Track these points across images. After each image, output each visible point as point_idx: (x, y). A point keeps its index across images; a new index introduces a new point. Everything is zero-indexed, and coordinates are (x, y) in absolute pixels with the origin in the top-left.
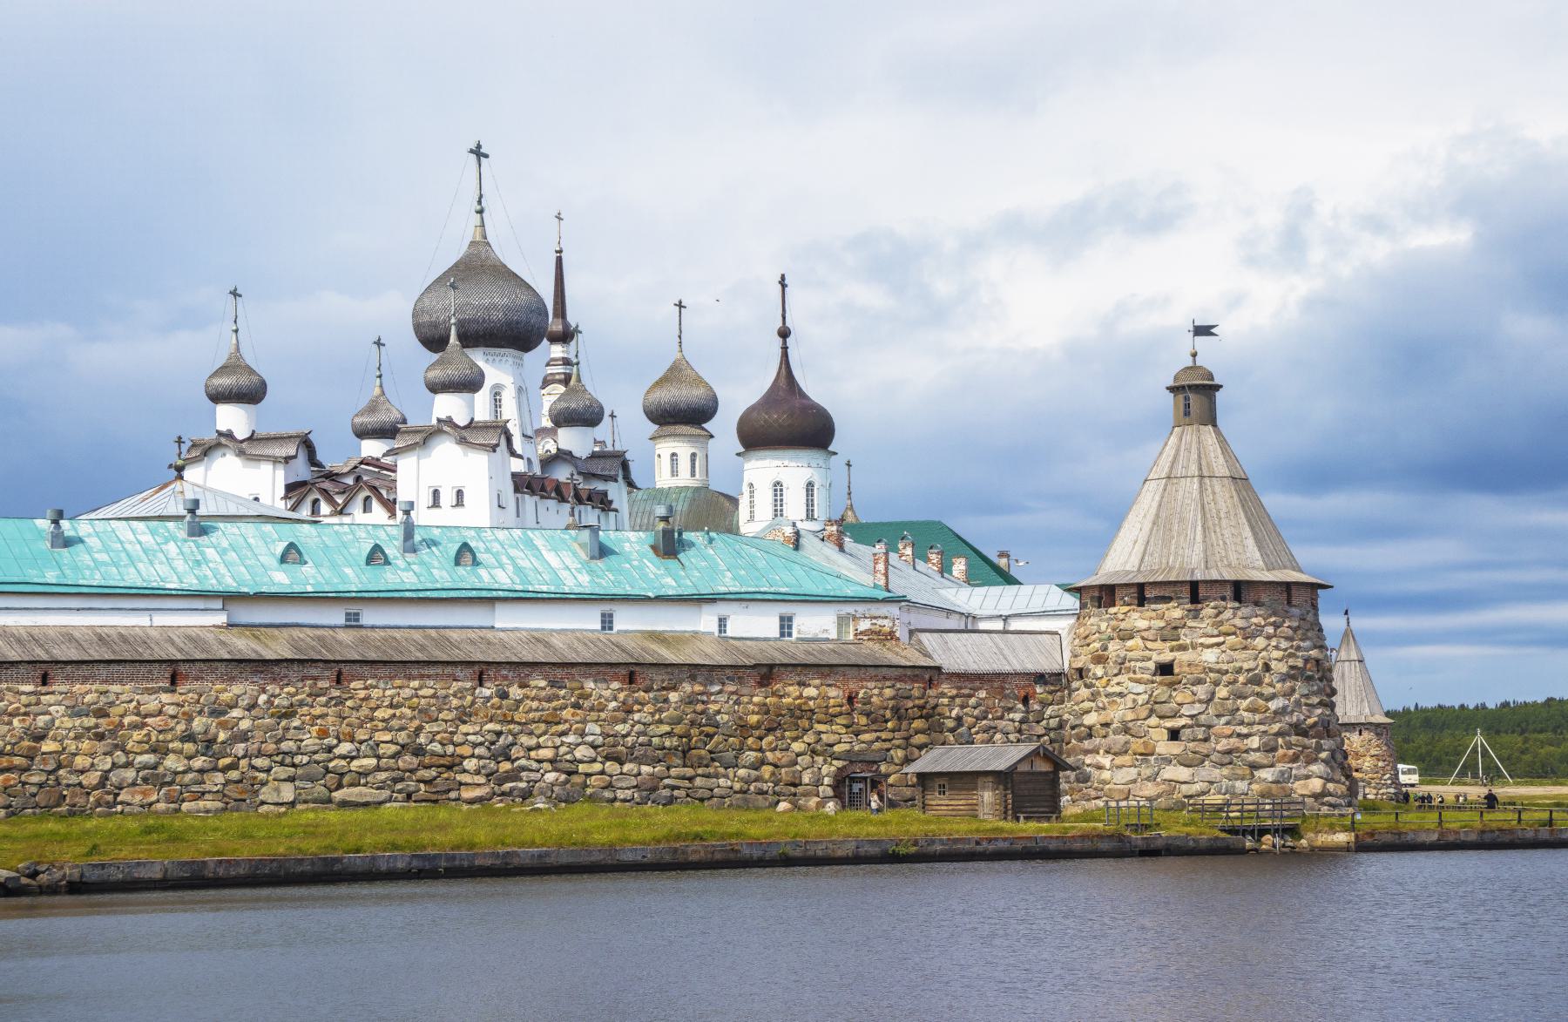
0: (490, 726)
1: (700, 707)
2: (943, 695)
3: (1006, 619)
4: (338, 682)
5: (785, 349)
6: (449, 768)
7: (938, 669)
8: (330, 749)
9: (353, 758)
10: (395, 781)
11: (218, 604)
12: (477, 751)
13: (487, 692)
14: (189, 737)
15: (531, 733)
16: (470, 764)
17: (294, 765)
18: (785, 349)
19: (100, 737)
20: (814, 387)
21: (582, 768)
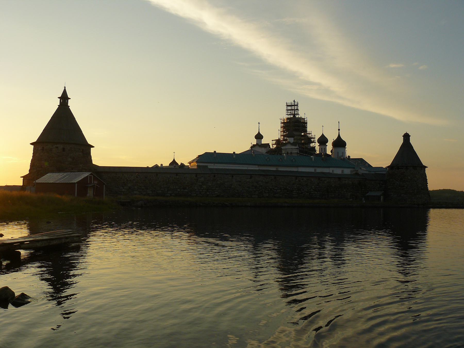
0: (298, 186)
4: (275, 178)
5: (339, 132)
8: (273, 188)
9: (277, 190)
11: (257, 166)
13: (297, 180)
18: (339, 132)
19: (240, 185)
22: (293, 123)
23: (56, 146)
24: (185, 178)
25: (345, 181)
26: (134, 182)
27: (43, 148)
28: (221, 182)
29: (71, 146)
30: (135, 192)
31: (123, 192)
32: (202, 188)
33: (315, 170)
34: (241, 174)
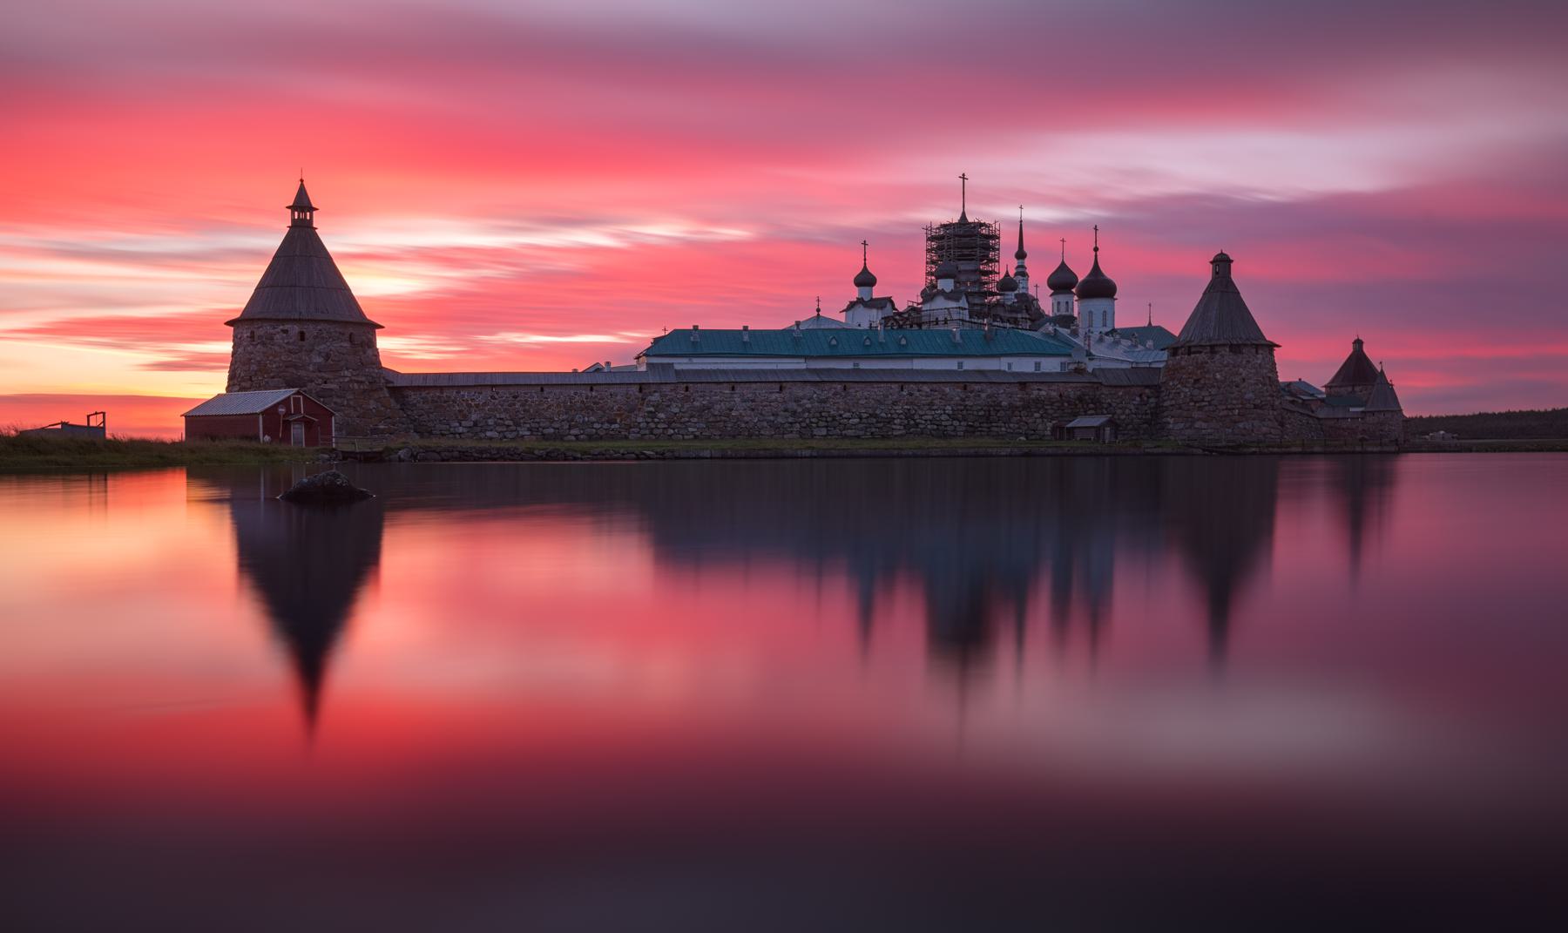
0: (906, 407)
1: (995, 399)
2: (1103, 394)
3: (1150, 363)
5: (1096, 256)
6: (889, 423)
7: (1101, 383)
8: (841, 415)
10: (867, 428)
11: (803, 360)
12: (902, 416)
14: (786, 410)
15: (922, 410)
16: (897, 421)
17: (827, 421)
18: (1096, 256)
19: (753, 410)
20: (1108, 272)
21: (943, 423)
22: (957, 238)
23: (281, 327)
24: (611, 395)
25: (1039, 389)
26: (486, 408)
27: (252, 333)
28: (704, 402)
29: (319, 327)
30: (489, 434)
31: (460, 434)
32: (656, 420)
33: (960, 365)
34: (756, 382)
